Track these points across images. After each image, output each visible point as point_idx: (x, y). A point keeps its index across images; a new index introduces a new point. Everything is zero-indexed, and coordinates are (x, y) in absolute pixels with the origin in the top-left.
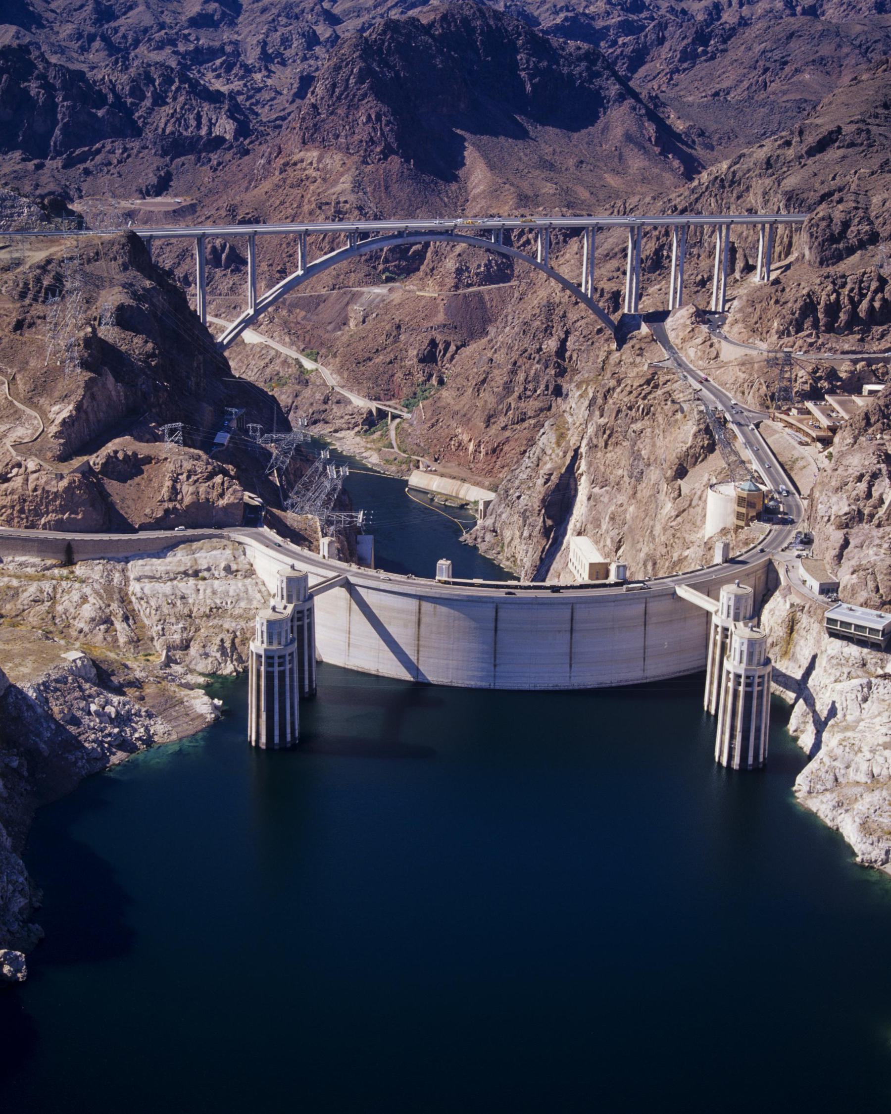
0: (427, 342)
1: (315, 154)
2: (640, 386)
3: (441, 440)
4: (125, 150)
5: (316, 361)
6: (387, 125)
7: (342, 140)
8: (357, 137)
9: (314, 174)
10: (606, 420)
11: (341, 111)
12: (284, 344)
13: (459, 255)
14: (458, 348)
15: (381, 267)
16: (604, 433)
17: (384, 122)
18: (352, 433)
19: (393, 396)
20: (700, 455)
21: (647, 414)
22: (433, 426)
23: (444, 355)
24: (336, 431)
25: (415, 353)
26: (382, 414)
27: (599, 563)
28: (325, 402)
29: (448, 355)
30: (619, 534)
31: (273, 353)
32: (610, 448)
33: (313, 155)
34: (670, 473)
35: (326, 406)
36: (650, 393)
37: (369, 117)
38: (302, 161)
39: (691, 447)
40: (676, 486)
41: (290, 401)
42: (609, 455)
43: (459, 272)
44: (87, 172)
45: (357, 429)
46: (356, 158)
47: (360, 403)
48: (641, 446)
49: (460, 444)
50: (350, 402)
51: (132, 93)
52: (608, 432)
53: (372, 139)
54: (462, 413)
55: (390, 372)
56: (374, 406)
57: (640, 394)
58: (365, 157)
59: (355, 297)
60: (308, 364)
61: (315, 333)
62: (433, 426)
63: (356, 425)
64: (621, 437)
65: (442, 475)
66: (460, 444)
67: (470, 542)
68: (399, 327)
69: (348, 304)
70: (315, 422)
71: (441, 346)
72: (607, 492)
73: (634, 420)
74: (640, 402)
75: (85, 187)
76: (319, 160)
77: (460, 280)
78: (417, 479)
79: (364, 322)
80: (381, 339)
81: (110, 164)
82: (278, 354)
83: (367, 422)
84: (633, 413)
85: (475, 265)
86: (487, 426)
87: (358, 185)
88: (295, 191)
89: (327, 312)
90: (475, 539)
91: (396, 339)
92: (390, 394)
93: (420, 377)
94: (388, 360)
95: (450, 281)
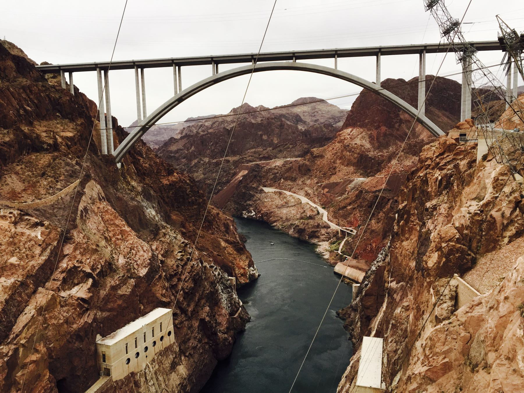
8: (367, 121)
12: (315, 202)
15: (369, 171)
20: (511, 222)
21: (445, 188)
24: (319, 242)
31: (308, 206)
33: (349, 130)
36: (449, 163)
39: (487, 204)
42: (405, 243)
44: (280, 151)
45: (330, 241)
47: (334, 226)
50: (330, 227)
56: (339, 228)
57: (439, 163)
59: (351, 181)
60: (321, 210)
63: (330, 239)
65: (352, 267)
73: (429, 198)
74: (438, 174)
75: (278, 156)
76: (351, 132)
81: (289, 148)
86: (383, 239)
87: (363, 138)
89: (338, 189)
92: (351, 224)
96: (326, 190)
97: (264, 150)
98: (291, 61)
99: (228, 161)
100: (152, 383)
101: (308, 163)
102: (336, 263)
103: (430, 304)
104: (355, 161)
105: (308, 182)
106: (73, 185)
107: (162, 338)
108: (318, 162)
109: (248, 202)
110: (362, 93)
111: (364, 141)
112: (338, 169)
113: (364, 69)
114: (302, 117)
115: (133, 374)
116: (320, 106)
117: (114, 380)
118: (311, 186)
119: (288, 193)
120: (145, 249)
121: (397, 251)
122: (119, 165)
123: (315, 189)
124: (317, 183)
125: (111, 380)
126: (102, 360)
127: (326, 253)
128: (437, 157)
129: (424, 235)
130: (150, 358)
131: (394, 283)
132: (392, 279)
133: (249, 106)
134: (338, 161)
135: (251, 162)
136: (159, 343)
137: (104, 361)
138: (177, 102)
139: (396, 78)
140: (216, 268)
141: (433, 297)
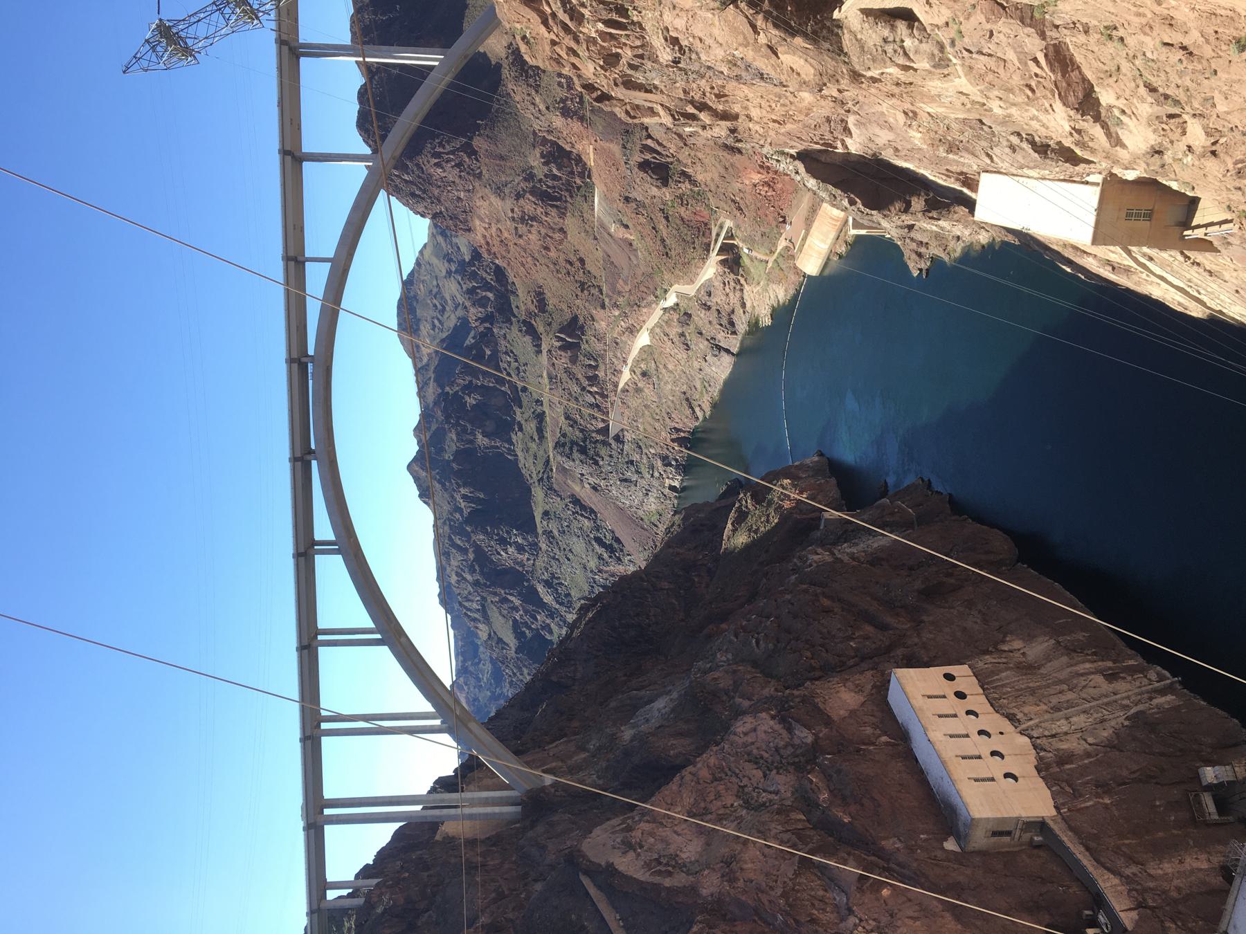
0: (642, 174)
1: (477, 222)
2: (545, 23)
3: (759, 205)
4: (506, 353)
5: (666, 291)
6: (444, 147)
7: (462, 195)
8: (457, 180)
9: (494, 229)
10: (659, 107)
11: (436, 192)
12: (650, 314)
13: (548, 108)
14: (649, 136)
15: (578, 181)
16: (693, 117)
17: (441, 150)
18: (747, 288)
19: (706, 224)
22: (740, 209)
23: (659, 153)
24: (743, 305)
25: (655, 189)
26: (725, 249)
27: (1100, 210)
28: (709, 308)
29: (658, 148)
30: (1013, 148)
31: (658, 330)
32: (736, 108)
34: (797, 59)
35: (714, 308)
37: (437, 165)
38: (485, 237)
40: (874, 35)
41: (706, 343)
42: (755, 113)
43: (566, 113)
45: (742, 281)
46: (477, 184)
47: (711, 269)
48: (719, 53)
49: (766, 184)
50: (710, 280)
51: (484, 306)
52: (690, 109)
53: (459, 165)
54: (722, 171)
55: (679, 222)
56: (714, 258)
57: (566, 28)
58: (474, 175)
59: (602, 226)
60: (671, 300)
61: (640, 278)
62: (740, 209)
64: (703, 83)
66: (766, 184)
67: (925, 265)
68: (627, 199)
69: (609, 234)
70: (732, 324)
71: (648, 156)
72: (859, 124)
74: (591, 29)
75: (535, 396)
76: (482, 220)
77: (575, 113)
78: (811, 265)
79: (626, 227)
80: (642, 220)
81: (518, 368)
82: (658, 325)
83: (735, 268)
84: (627, 54)
85: (559, 89)
87: (499, 191)
88: (512, 248)
89: (619, 258)
90: (920, 255)
91: (640, 204)
93: (685, 187)
94: (664, 222)
95: (576, 126)
96: (620, 285)
97: (521, 429)
98: (310, 365)
99: (546, 513)
100: (1063, 721)
101: (555, 326)
102: (795, 268)
103: (903, 78)
104: (554, 212)
105: (602, 325)
106: (593, 891)
107: (960, 695)
108: (551, 302)
109: (644, 470)
110: (395, 191)
111: (507, 191)
112: (573, 258)
113: (333, 190)
114: (444, 335)
115: (1042, 768)
116: (421, 290)
117: (1054, 812)
118: (612, 324)
119: (626, 376)
120: (748, 726)
121: (772, 133)
122: (549, 779)
123: (617, 313)
124: (603, 307)
125: (1053, 819)
126: (1007, 839)
127: (771, 292)
128: (549, 29)
129: (736, 71)
130: (1006, 725)
131: (849, 141)
132: (839, 145)
133: (415, 460)
134: (553, 254)
135: (548, 461)
136: (970, 703)
137: (1008, 833)
138: (403, 640)
139: (356, 107)
140: (800, 558)
141: (888, 70)
